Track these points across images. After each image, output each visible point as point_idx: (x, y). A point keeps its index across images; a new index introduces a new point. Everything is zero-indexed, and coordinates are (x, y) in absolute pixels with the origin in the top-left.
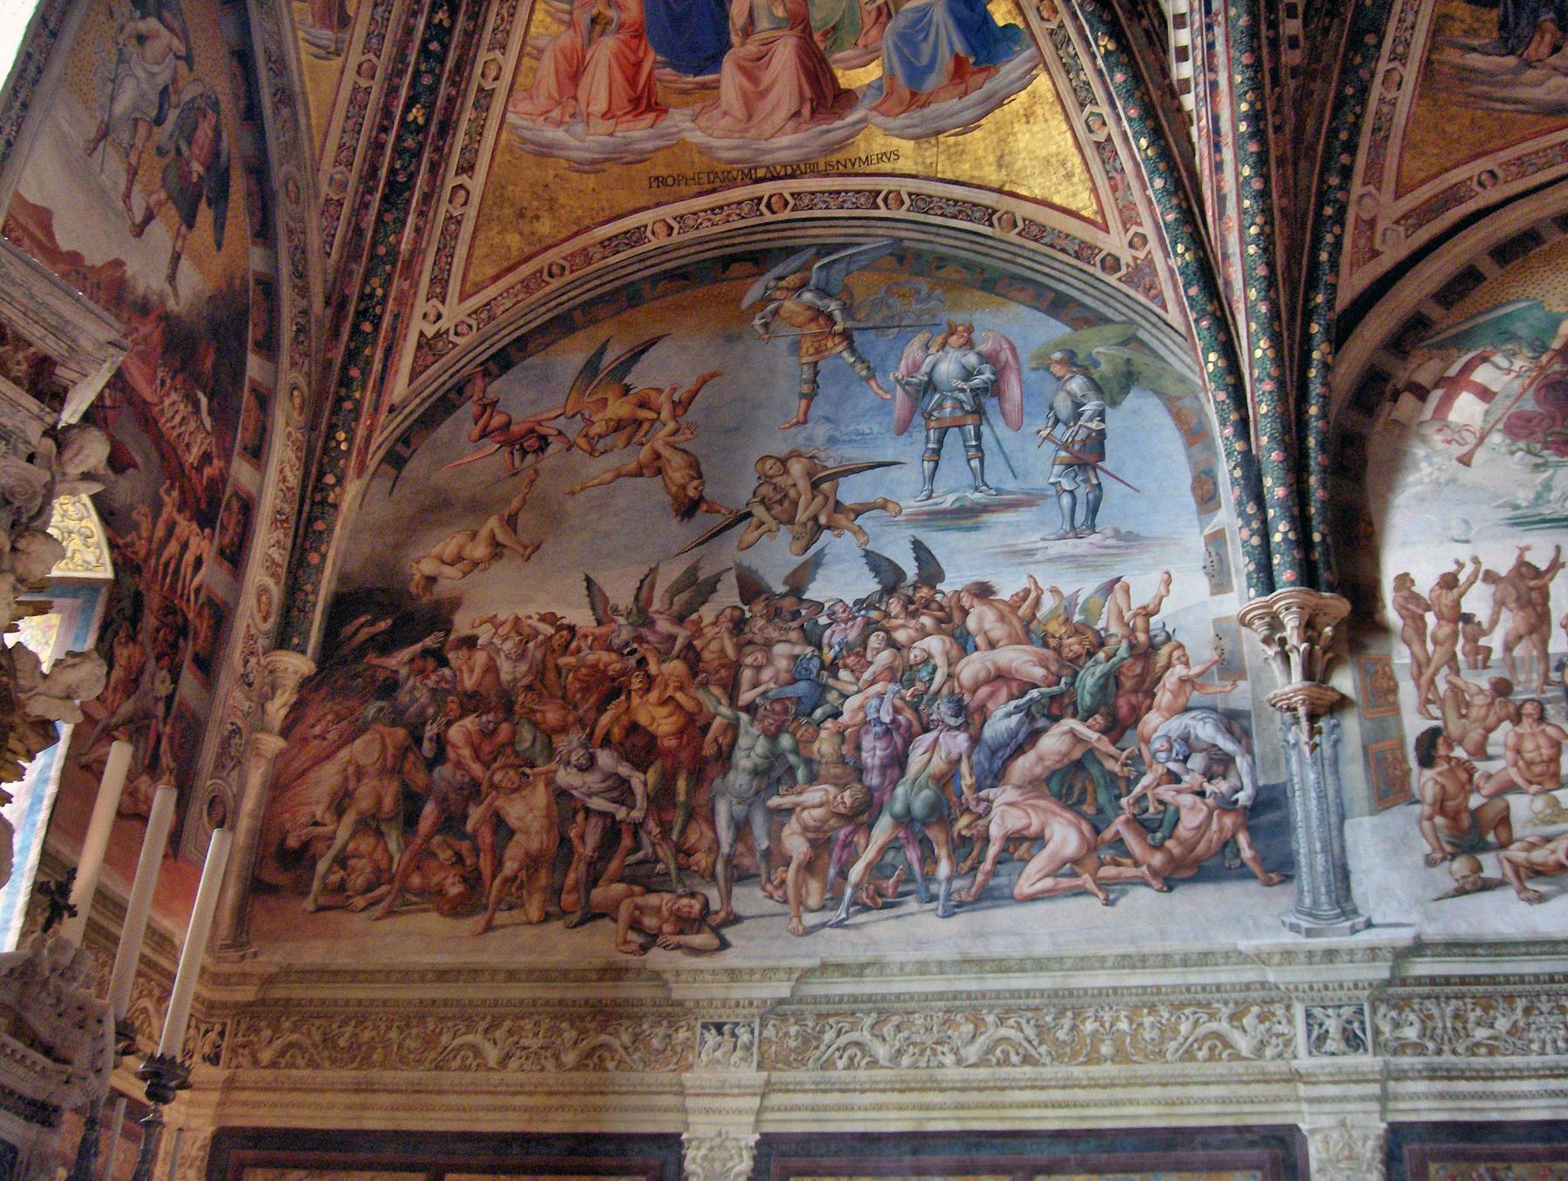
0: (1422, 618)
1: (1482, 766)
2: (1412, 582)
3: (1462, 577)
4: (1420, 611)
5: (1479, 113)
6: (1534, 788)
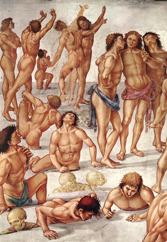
0: (15, 51)
1: (35, 153)
2: (13, 24)
3: (43, 24)
4: (14, 46)
6: (63, 168)
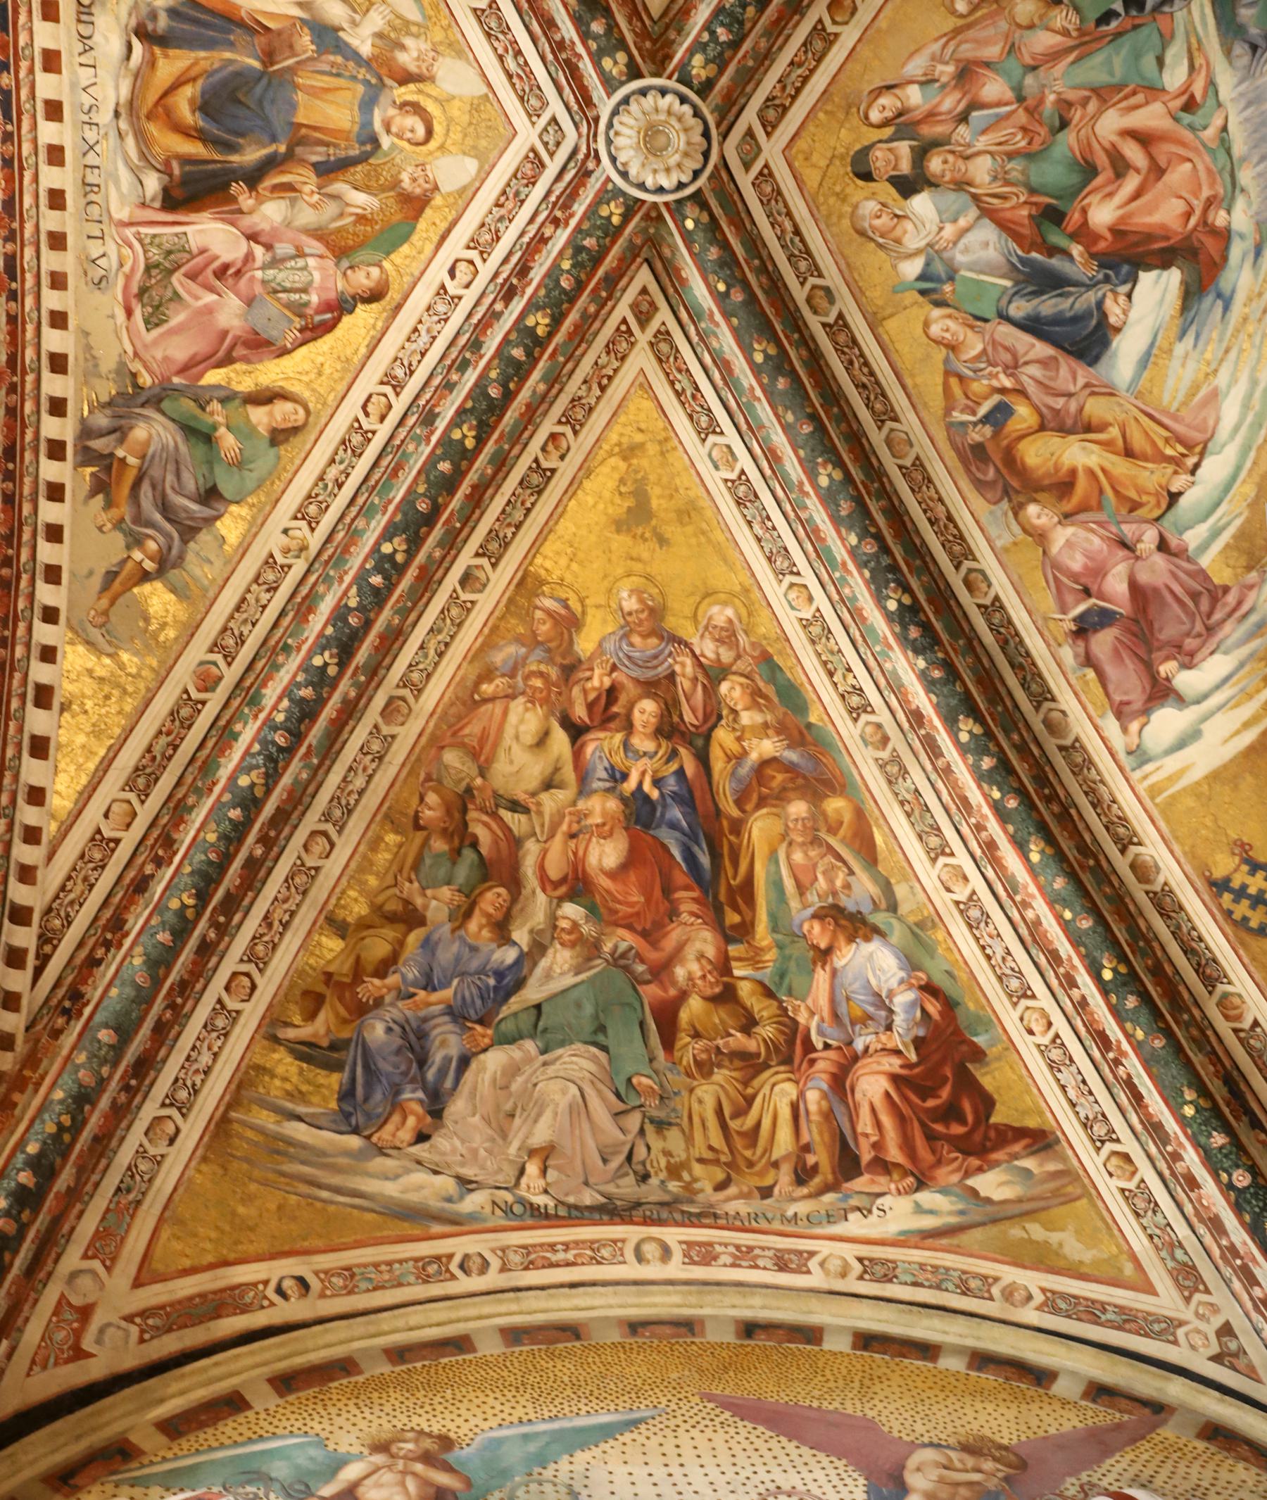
5: (293, 1199)
